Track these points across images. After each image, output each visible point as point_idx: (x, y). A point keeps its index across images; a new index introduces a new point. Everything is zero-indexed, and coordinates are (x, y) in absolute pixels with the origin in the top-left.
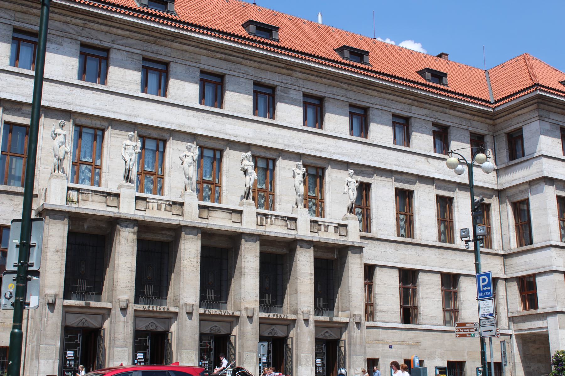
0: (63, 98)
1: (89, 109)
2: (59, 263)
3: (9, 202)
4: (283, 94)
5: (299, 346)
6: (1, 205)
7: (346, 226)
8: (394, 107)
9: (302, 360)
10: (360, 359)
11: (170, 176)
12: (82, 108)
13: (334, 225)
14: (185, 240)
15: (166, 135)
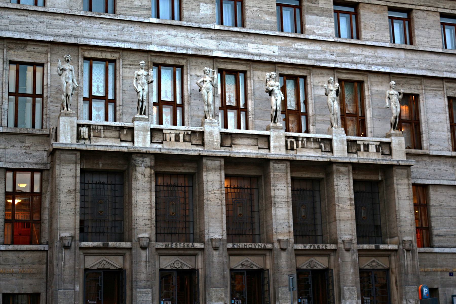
0: (69, 31)
1: (97, 41)
2: (73, 204)
3: (21, 144)
4: (310, 4)
5: (341, 278)
6: (12, 148)
7: (389, 143)
8: (442, 6)
9: (345, 293)
10: (413, 290)
11: (189, 104)
12: (90, 40)
13: (375, 143)
14: (207, 171)
15: (183, 62)
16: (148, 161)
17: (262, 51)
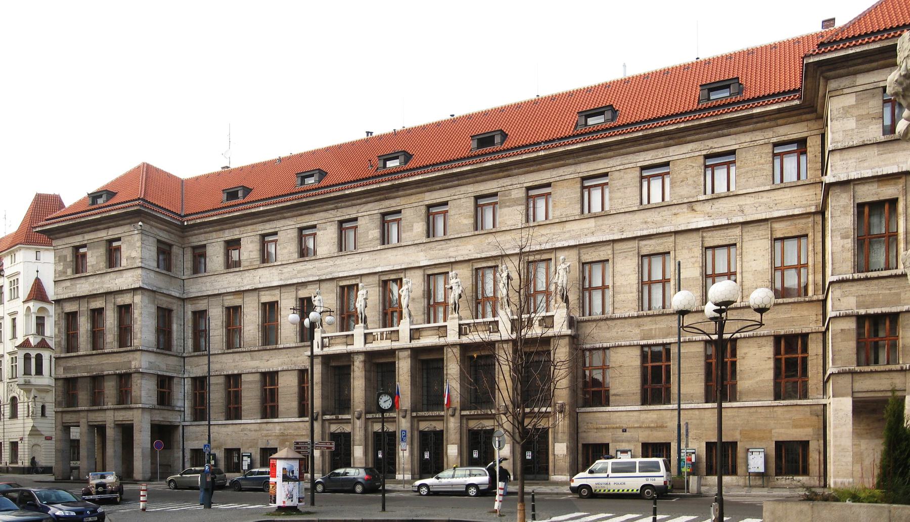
15: (402, 275)
16: (362, 358)
17: (460, 252)
